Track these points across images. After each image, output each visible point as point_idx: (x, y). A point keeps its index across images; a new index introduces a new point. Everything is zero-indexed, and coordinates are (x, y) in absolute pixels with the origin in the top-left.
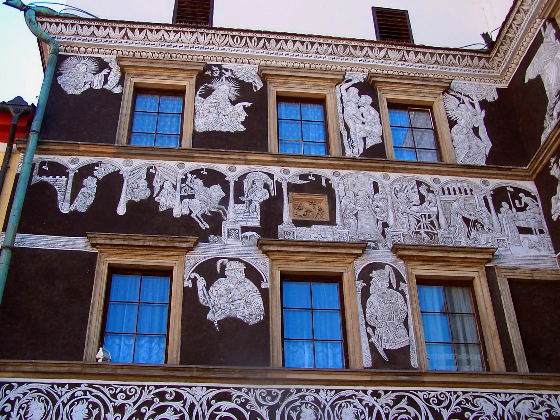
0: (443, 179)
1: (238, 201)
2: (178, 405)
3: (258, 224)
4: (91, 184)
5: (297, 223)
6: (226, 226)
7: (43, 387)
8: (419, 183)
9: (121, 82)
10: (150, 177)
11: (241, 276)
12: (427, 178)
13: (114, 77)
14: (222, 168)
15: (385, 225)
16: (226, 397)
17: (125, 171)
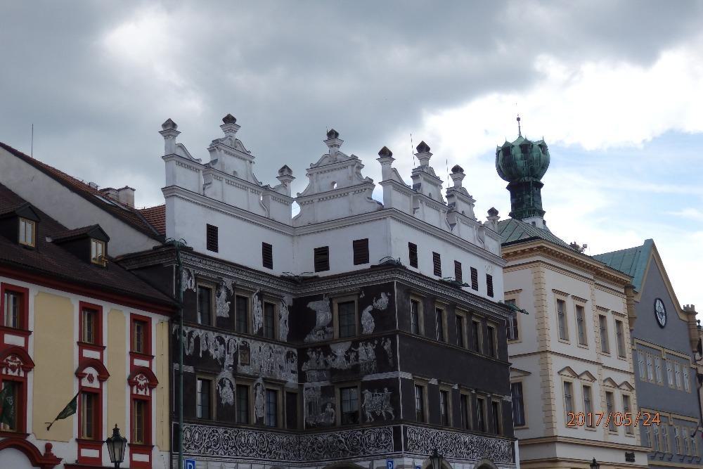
0: (276, 346)
1: (228, 353)
2: (217, 434)
3: (232, 364)
4: (192, 340)
5: (243, 364)
6: (226, 364)
7: (189, 426)
8: (270, 348)
9: (195, 286)
10: (207, 338)
11: (228, 386)
12: (272, 345)
13: (193, 283)
14: (223, 336)
15: (261, 366)
16: (226, 432)
17: (200, 334)
